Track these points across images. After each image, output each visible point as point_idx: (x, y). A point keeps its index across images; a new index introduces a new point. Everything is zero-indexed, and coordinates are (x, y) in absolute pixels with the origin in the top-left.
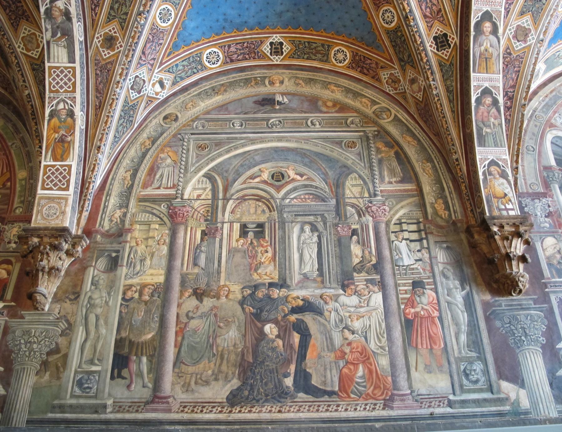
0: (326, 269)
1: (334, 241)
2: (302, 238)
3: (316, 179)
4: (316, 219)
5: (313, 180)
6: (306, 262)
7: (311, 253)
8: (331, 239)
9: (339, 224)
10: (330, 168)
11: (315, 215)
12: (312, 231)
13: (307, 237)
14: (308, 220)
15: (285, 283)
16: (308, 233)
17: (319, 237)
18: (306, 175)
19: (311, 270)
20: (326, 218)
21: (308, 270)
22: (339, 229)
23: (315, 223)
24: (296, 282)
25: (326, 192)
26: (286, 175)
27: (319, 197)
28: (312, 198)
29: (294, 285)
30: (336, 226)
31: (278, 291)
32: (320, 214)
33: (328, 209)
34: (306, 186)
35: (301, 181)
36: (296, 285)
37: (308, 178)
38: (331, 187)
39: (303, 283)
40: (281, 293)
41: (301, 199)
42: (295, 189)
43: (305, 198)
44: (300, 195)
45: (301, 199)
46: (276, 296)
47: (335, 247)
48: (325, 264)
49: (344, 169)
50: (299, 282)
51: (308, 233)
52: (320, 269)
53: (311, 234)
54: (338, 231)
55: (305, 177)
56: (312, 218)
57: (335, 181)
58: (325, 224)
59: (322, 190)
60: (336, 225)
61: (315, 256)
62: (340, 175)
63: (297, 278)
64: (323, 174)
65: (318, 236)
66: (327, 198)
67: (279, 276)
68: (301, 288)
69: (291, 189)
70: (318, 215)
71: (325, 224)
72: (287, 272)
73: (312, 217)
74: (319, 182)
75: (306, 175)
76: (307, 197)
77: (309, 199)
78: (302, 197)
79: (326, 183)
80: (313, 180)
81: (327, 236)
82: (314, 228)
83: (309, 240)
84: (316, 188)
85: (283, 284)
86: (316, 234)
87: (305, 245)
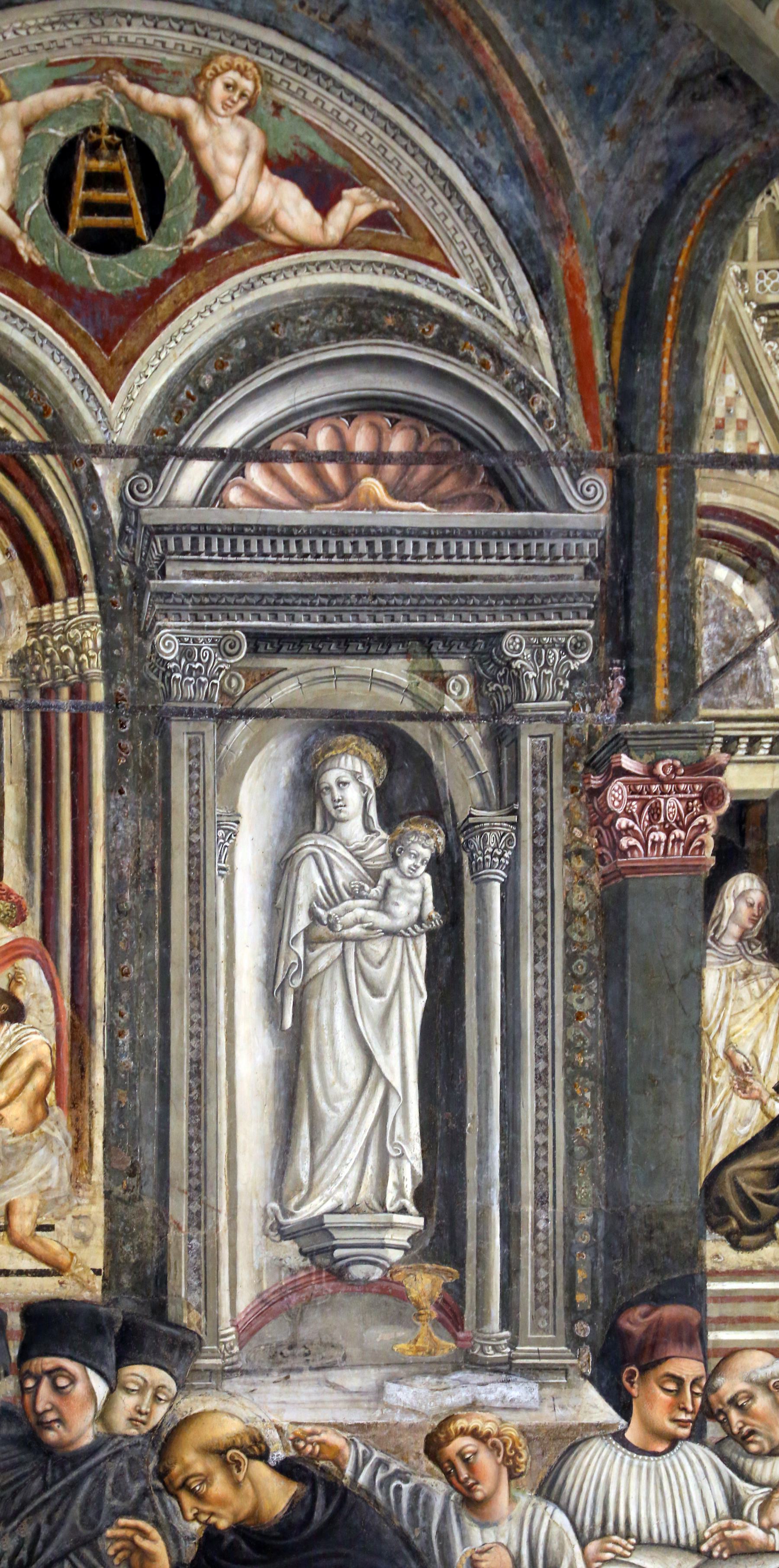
0: (483, 1190)
1: (571, 914)
2: (309, 882)
3: (458, 242)
4: (429, 691)
5: (427, 250)
6: (332, 1119)
7: (370, 1040)
8: (542, 903)
9: (619, 743)
10: (595, 94)
11: (425, 643)
12: (391, 811)
13: (345, 874)
14: (358, 699)
15: (159, 1310)
16: (353, 830)
17: (447, 874)
18: (366, 177)
19: (366, 1193)
20: (515, 679)
21: (343, 1195)
22: (617, 794)
23: (419, 732)
24: (245, 1300)
25: (527, 389)
26: (178, 172)
27: (468, 441)
28: (408, 460)
29: (227, 1329)
30: (592, 766)
31: (101, 1388)
32: (468, 638)
33: (540, 579)
34: (361, 314)
35: (316, 245)
36: (247, 1332)
37: (378, 219)
38: (580, 324)
39: (297, 1317)
40: (126, 1403)
41: (310, 460)
42: (256, 348)
43: (343, 455)
44: (301, 420)
45: (310, 460)
46: (82, 1430)
47: (572, 980)
48: (483, 1146)
49: (719, 114)
50: (268, 1307)
51: (353, 830)
52: (441, 1192)
53: (378, 847)
54: (602, 819)
55: (353, 206)
56: (385, 681)
57: (624, 257)
58: (502, 740)
59: (502, 361)
60: (593, 760)
61: (400, 1059)
62: (677, 182)
63: (249, 1265)
64: (522, 169)
65: (435, 866)
66: (541, 462)
67: (111, 1247)
68: (290, 1359)
69: (220, 348)
70: (450, 641)
71: (502, 740)
72: (179, 1208)
73: (394, 668)
74: (477, 283)
75: (366, 177)
76: (361, 440)
77: (377, 459)
78: (322, 439)
79: (540, 288)
80: (427, 250)
81: (513, 868)
82: (409, 792)
83: (358, 909)
84: (451, 335)
85: (135, 1318)
86: (424, 844)
87: (325, 957)
